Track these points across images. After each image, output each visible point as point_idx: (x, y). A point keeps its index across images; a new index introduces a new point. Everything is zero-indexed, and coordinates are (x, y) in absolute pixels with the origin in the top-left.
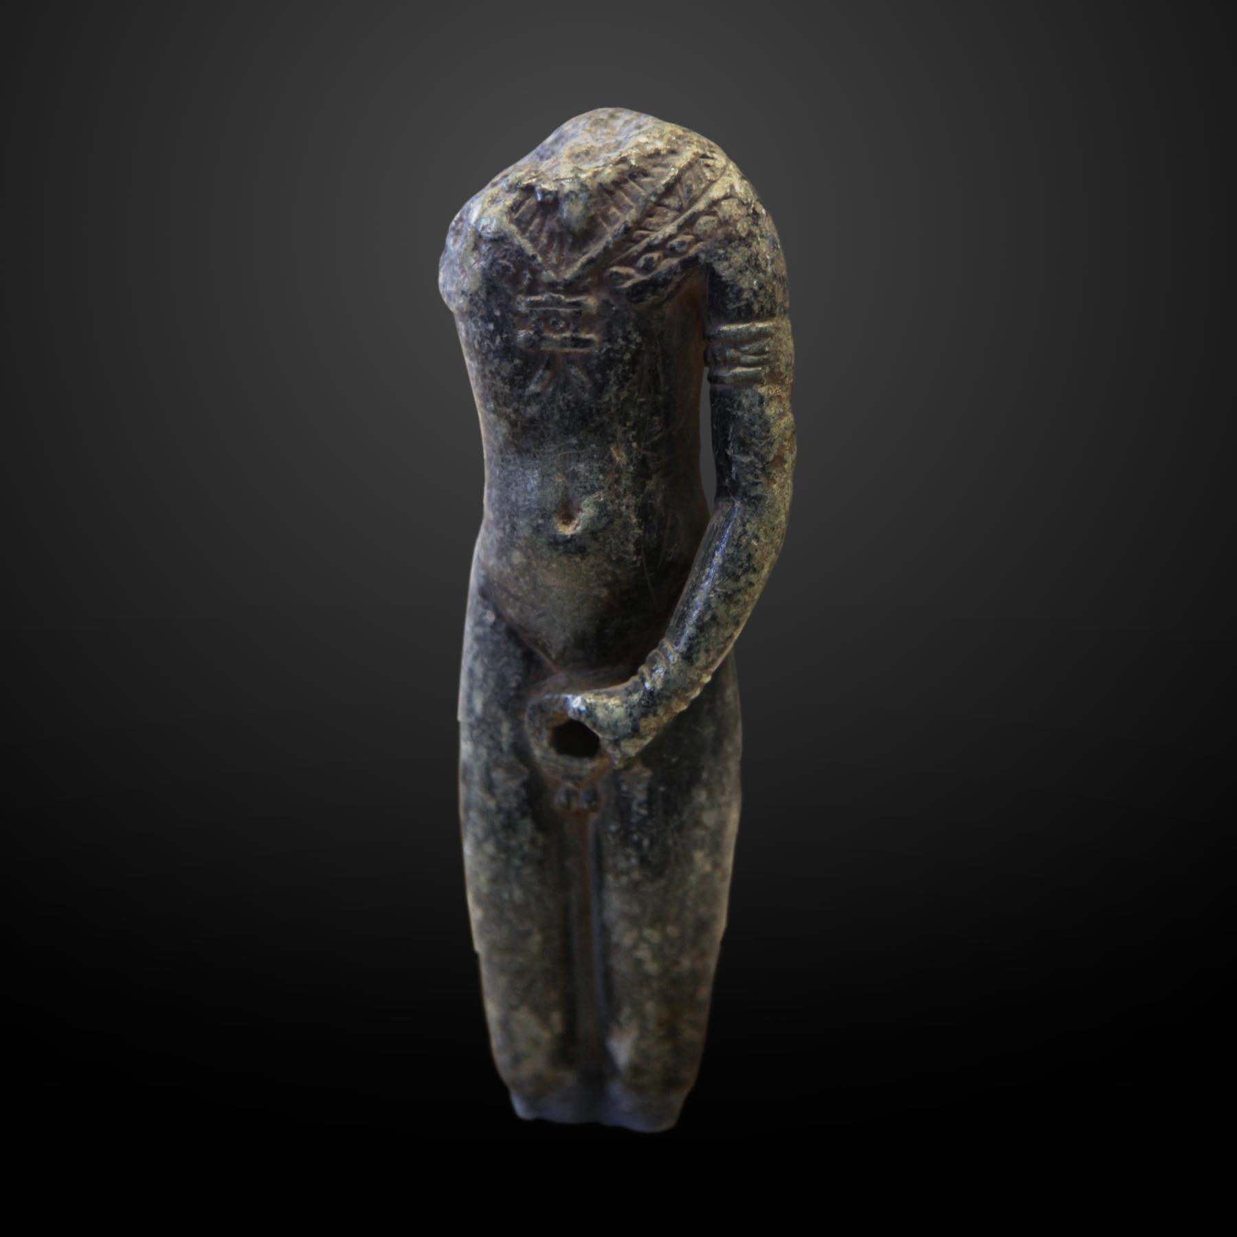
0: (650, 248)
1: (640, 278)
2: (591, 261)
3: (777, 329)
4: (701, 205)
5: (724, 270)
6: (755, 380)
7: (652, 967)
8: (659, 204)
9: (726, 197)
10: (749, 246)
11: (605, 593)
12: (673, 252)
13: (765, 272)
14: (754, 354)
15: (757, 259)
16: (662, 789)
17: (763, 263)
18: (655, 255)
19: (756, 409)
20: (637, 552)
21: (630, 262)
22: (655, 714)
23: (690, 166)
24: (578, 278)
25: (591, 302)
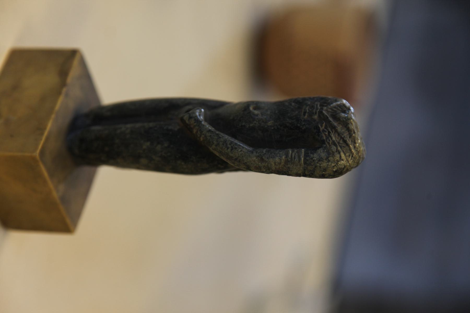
0: (329, 132)
1: (321, 129)
2: (327, 117)
3: (300, 165)
4: (339, 148)
5: (320, 151)
6: (287, 156)
7: (118, 131)
8: (341, 138)
9: (340, 157)
10: (326, 159)
11: (231, 118)
12: (327, 138)
13: (317, 163)
14: (294, 156)
15: (322, 161)
16: (171, 133)
17: (320, 163)
18: (327, 133)
19: (278, 155)
20: (242, 126)
21: (326, 127)
22: (195, 122)
23: (350, 150)
24: (323, 114)
25: (316, 117)
